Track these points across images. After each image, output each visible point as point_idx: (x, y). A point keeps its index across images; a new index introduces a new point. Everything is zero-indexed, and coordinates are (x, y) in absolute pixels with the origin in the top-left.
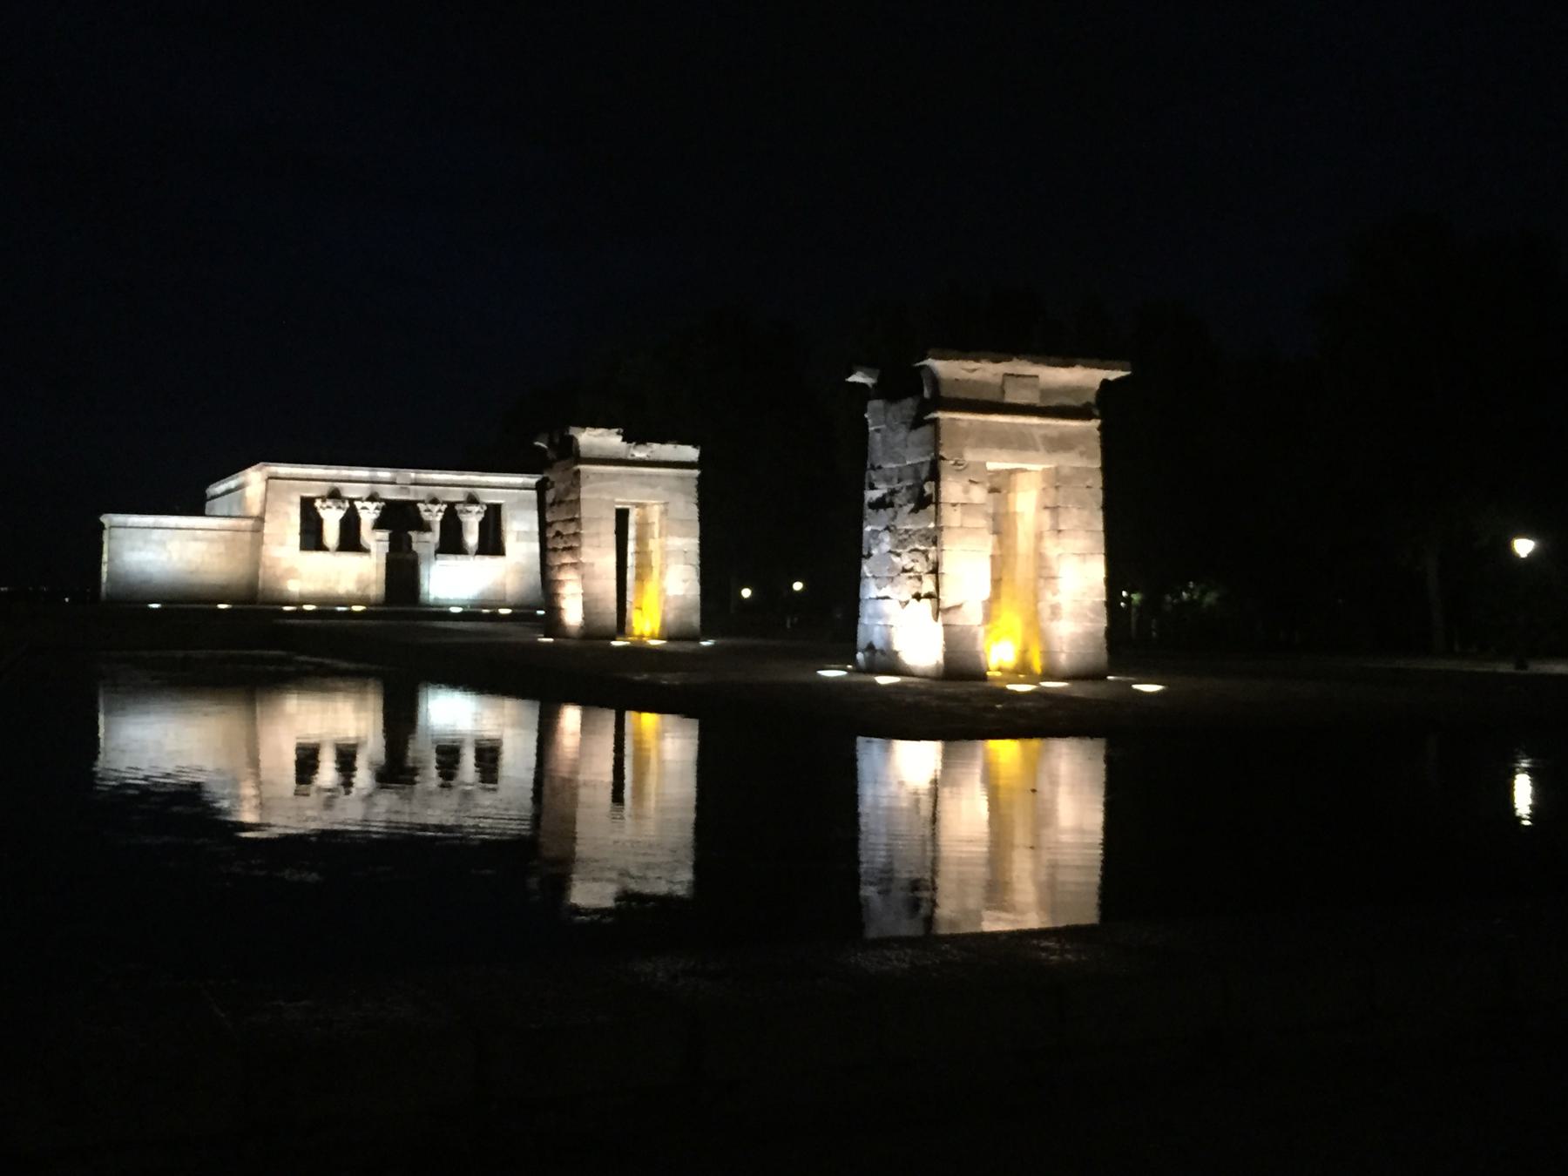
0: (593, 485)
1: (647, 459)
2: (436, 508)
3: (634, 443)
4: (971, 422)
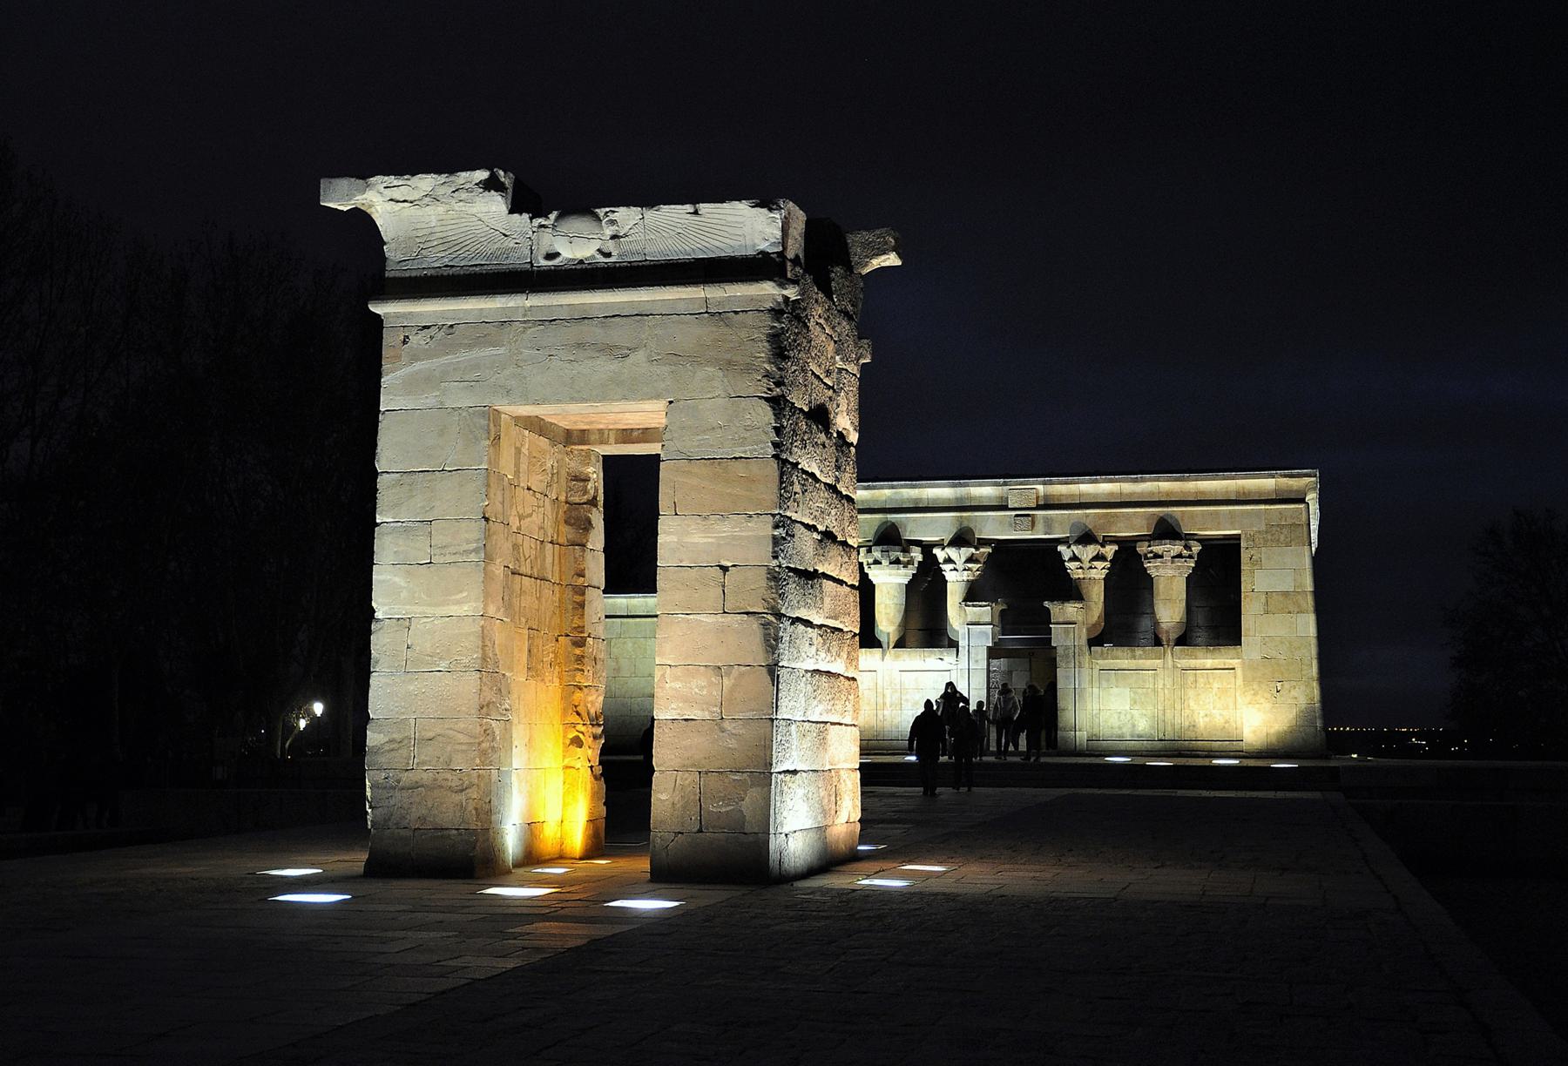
0: (418, 366)
1: (601, 259)
2: (1091, 550)
3: (553, 216)
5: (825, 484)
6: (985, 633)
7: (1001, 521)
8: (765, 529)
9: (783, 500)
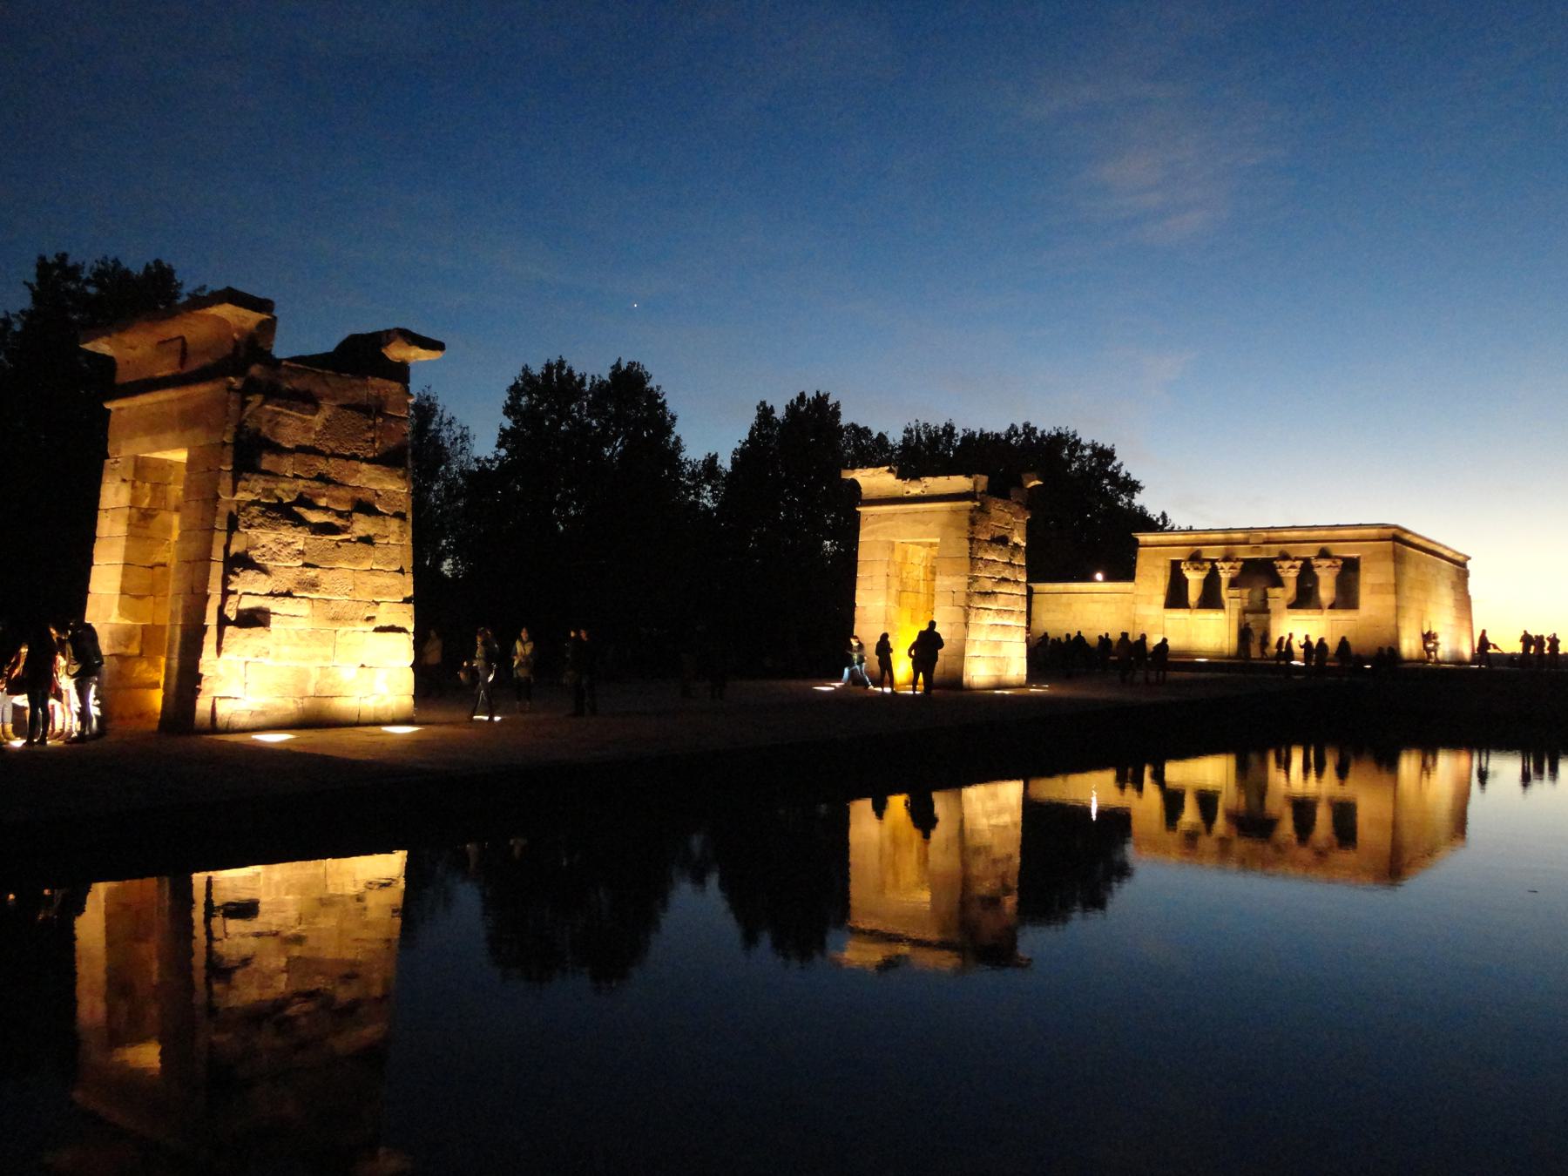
0: (870, 527)
2: (1286, 564)
3: (908, 480)
4: (130, 408)
5: (1004, 563)
6: (1237, 602)
7: (1246, 549)
8: (966, 580)
9: (972, 570)
